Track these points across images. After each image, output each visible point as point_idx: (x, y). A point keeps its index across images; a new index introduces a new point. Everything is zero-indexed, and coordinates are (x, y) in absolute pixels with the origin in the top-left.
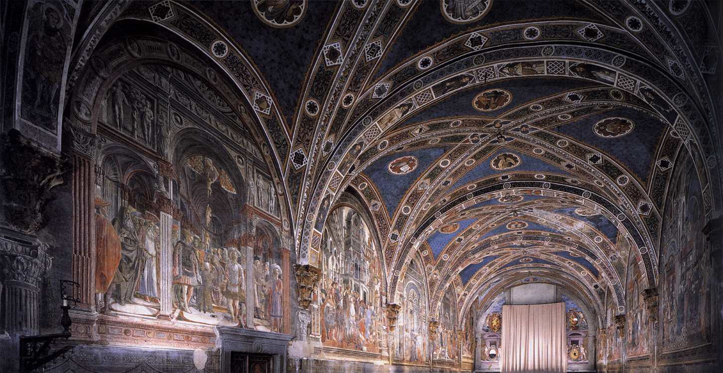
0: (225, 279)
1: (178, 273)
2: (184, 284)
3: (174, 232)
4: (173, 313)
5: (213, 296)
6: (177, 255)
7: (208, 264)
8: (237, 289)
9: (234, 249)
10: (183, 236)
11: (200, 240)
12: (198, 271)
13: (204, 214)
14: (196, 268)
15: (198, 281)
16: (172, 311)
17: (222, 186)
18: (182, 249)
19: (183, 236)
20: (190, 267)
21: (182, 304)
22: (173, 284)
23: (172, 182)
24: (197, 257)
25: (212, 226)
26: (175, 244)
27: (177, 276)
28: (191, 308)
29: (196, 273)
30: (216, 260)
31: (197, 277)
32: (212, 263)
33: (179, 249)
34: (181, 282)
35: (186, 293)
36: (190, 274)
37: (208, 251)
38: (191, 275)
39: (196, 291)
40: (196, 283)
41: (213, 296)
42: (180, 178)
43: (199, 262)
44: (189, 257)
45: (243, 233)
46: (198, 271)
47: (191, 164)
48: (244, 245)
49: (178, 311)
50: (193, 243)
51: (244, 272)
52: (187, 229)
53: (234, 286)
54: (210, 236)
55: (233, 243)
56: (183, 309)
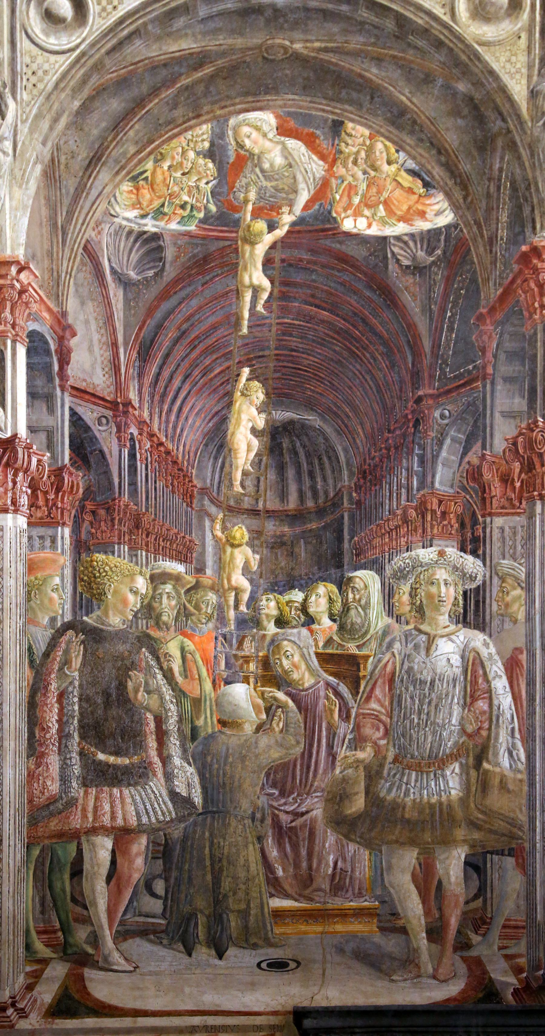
0: (358, 742)
1: (54, 787)
2: (94, 831)
3: (32, 591)
4: (30, 988)
5: (274, 853)
6: (52, 699)
7: (241, 694)
8: (452, 783)
9: (426, 554)
10: (89, 591)
11: (190, 580)
12: (174, 745)
13: (218, 440)
14: (161, 735)
15: (174, 795)
16: (21, 980)
17: (348, 225)
18: (77, 662)
19: (89, 591)
20: (130, 738)
21: (81, 934)
22: (29, 847)
23: (22, 351)
24: (168, 675)
25: (272, 476)
26: (41, 647)
27: (53, 800)
28: (139, 947)
29: (165, 760)
30: (299, 657)
31: (169, 777)
32: (270, 675)
33: (67, 662)
34: (76, 822)
35: (104, 871)
36: (127, 771)
37: (242, 622)
38: (136, 775)
39: (164, 852)
40: (165, 809)
41: (274, 853)
42: (72, 304)
43: (179, 693)
44: (122, 686)
45: (502, 433)
46: (174, 745)
47: (137, 204)
48: (510, 508)
49: (58, 971)
50: (149, 610)
51: (511, 666)
52: (106, 548)
53: (436, 763)
54: (256, 537)
55: (422, 520)
56: (81, 960)
